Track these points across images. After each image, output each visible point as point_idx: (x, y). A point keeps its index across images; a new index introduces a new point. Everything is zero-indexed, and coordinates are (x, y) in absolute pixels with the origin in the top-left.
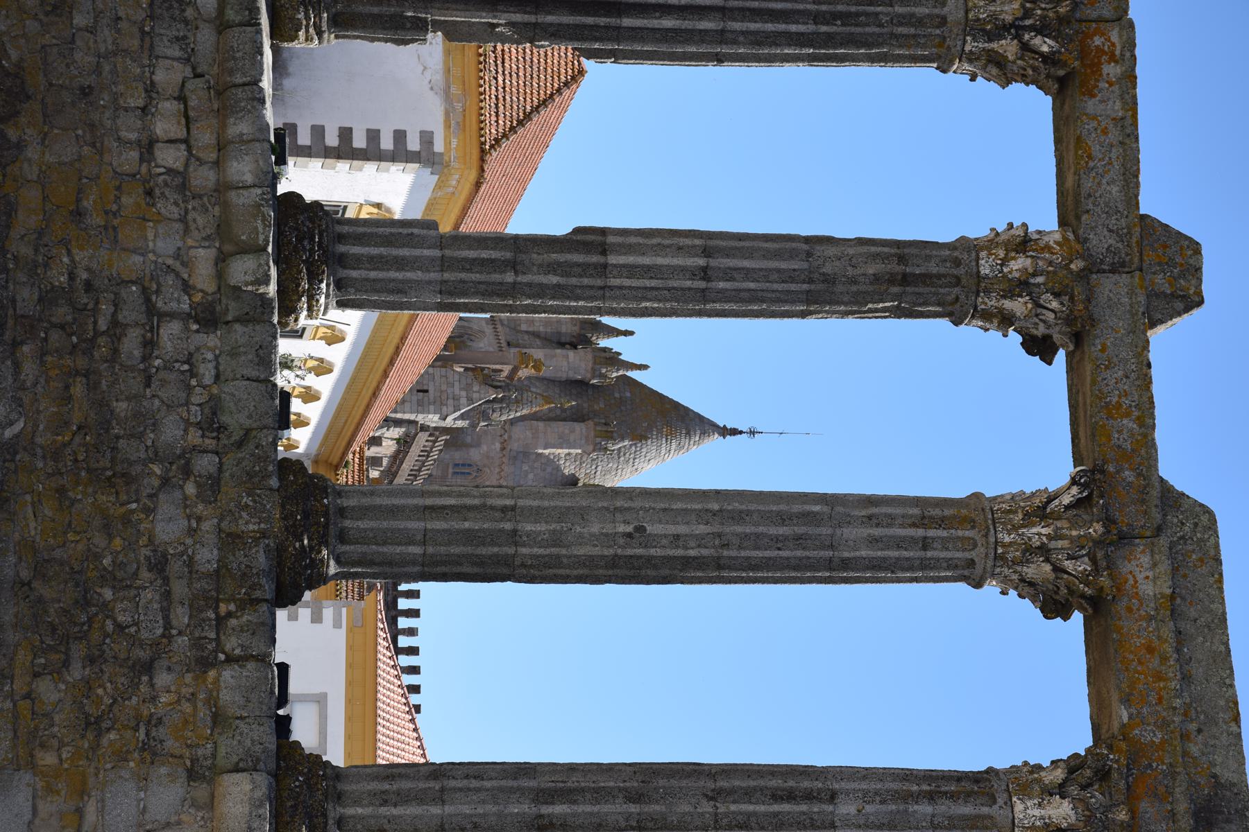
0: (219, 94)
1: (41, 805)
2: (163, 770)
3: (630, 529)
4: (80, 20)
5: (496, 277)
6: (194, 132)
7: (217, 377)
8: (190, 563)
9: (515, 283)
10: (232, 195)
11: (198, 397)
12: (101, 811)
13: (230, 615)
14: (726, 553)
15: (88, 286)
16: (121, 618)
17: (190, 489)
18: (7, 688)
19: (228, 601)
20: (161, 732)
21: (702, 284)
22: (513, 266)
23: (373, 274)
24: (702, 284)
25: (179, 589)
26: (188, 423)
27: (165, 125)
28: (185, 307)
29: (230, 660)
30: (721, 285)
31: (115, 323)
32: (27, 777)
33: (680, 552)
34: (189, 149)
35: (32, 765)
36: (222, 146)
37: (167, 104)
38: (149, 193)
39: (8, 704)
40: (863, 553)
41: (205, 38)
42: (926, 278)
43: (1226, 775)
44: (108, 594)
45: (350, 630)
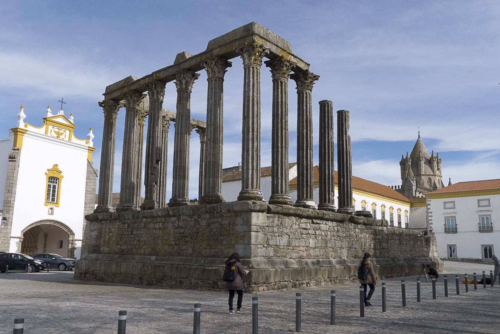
0: (154, 218)
1: (240, 243)
2: (236, 221)
3: (209, 141)
4: (146, 240)
5: (178, 170)
6: (158, 221)
7: (186, 216)
8: (208, 219)
9: (179, 167)
10: (163, 215)
11: (188, 219)
12: (241, 232)
13: (216, 212)
14: (213, 124)
15: (175, 238)
16: (215, 231)
17: (200, 220)
18: (223, 250)
19: (214, 212)
20: (231, 223)
21: (180, 134)
22: (177, 167)
23: (177, 191)
24: (180, 134)
25: (212, 220)
26: (191, 221)
27: (157, 226)
28: (177, 222)
29: (221, 211)
30: (180, 131)
31: (179, 234)
32: (235, 245)
33: (212, 132)
34: (160, 222)
35: (234, 245)
36: (160, 217)
37: (155, 226)
38: (165, 228)
39: (226, 249)
40: (213, 99)
41: (149, 220)
42: (180, 97)
43: (243, 29)
44: (212, 233)
45: (431, 199)
